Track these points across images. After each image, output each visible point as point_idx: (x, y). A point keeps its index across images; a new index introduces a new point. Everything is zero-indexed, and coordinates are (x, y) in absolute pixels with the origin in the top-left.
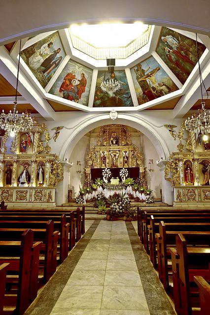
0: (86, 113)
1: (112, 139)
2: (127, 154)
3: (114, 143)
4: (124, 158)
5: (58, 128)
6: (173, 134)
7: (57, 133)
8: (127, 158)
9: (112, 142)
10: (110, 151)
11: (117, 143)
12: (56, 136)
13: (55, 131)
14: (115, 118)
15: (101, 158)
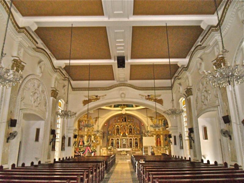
0: (109, 110)
1: (122, 118)
2: (131, 127)
3: (124, 120)
4: (129, 130)
5: (97, 118)
6: (152, 121)
7: (96, 120)
8: (131, 129)
9: (123, 120)
10: (121, 125)
11: (125, 121)
12: (96, 122)
13: (95, 119)
14: (125, 113)
15: (117, 129)
